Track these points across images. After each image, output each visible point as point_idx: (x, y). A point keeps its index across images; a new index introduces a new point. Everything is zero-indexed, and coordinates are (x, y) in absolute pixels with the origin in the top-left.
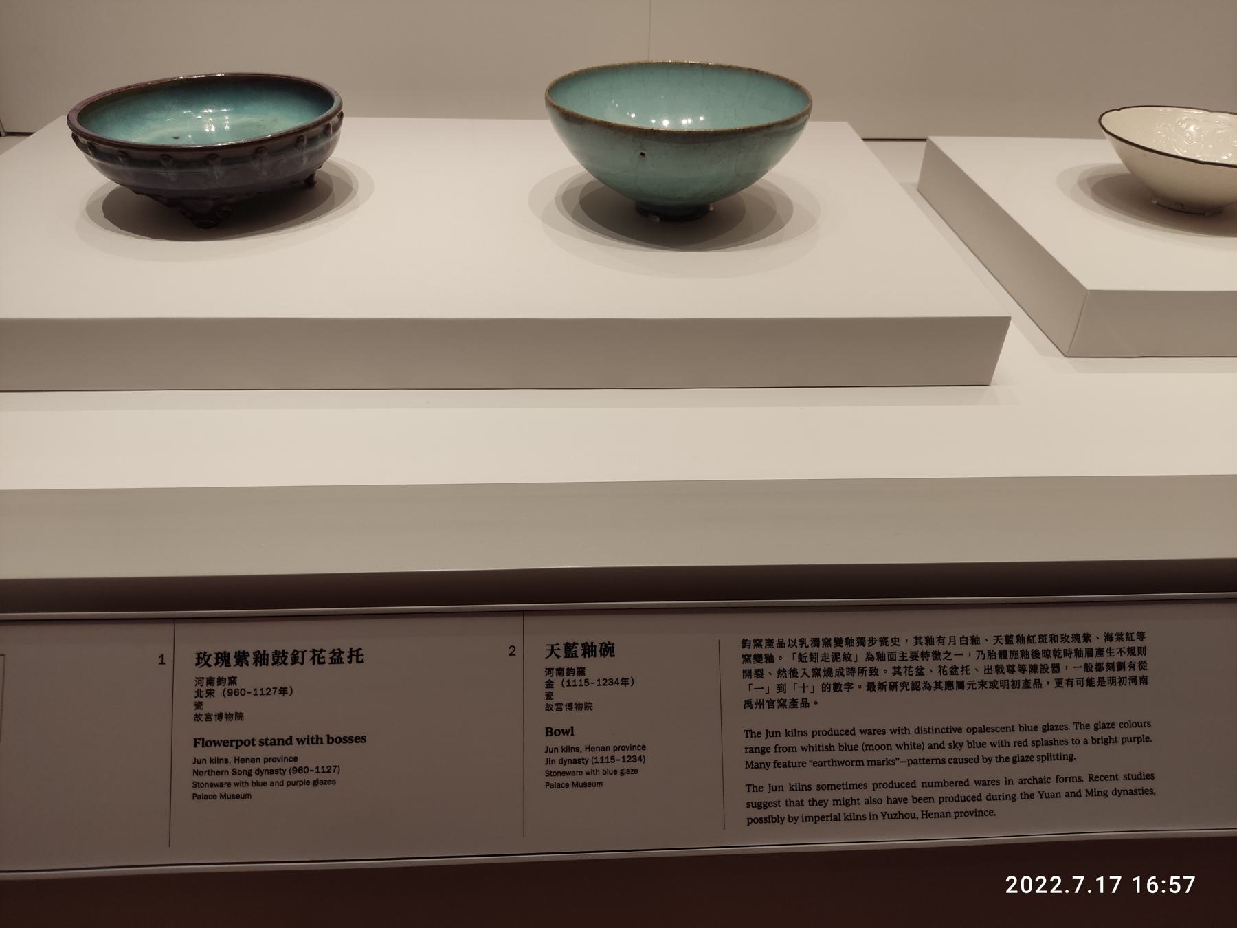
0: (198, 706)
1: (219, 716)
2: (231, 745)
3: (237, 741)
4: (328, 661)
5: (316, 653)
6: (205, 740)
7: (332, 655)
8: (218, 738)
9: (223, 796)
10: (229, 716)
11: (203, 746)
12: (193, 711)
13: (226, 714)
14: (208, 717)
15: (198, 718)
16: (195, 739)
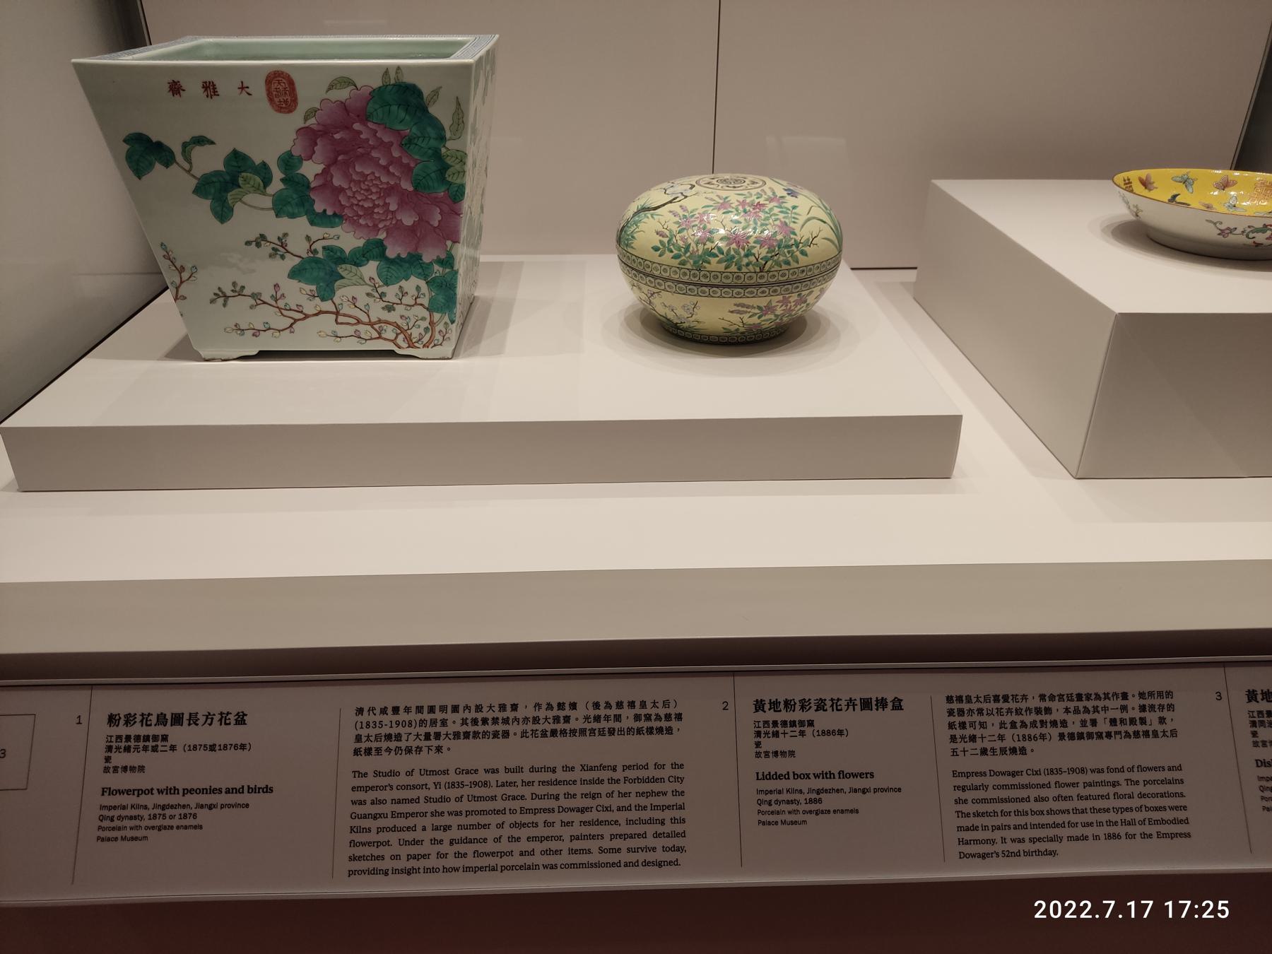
0: (108, 759)
1: (125, 769)
2: (134, 794)
3: (139, 790)
4: (233, 722)
5: (224, 715)
6: (112, 790)
7: (237, 717)
8: (122, 788)
9: (124, 839)
10: (133, 769)
11: (109, 795)
12: (103, 764)
13: (130, 767)
14: (116, 769)
15: (106, 770)
16: (103, 789)
